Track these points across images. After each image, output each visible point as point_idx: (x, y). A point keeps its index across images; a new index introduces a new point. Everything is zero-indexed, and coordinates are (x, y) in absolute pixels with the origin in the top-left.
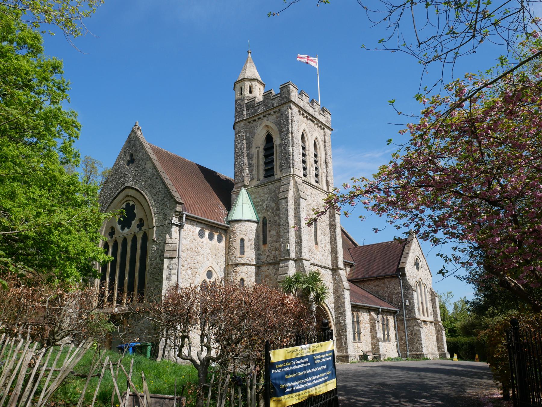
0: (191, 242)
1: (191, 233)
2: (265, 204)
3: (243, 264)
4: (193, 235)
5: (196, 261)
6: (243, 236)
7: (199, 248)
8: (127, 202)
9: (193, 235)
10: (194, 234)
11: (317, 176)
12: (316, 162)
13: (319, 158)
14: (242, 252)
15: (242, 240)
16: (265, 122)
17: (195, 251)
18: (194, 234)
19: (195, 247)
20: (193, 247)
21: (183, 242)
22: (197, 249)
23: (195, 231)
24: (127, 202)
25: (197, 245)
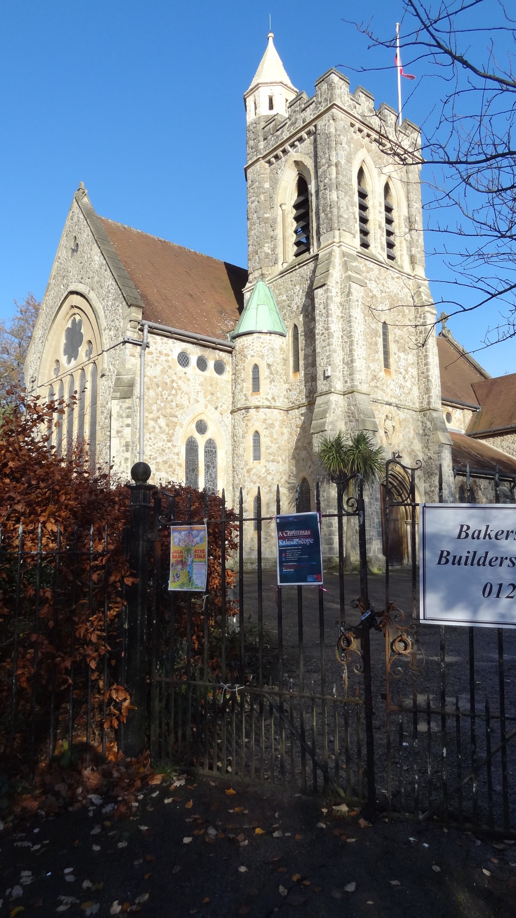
0: (164, 372)
1: (163, 358)
2: (294, 302)
3: (257, 407)
4: (167, 361)
5: (174, 404)
6: (256, 360)
7: (180, 382)
8: (72, 318)
9: (167, 361)
10: (169, 358)
11: (390, 245)
12: (389, 221)
13: (394, 214)
14: (256, 387)
15: (256, 368)
16: (294, 155)
17: (173, 387)
18: (169, 358)
19: (173, 381)
20: (168, 381)
21: (149, 372)
22: (175, 385)
23: (170, 353)
24: (72, 318)
25: (174, 377)
